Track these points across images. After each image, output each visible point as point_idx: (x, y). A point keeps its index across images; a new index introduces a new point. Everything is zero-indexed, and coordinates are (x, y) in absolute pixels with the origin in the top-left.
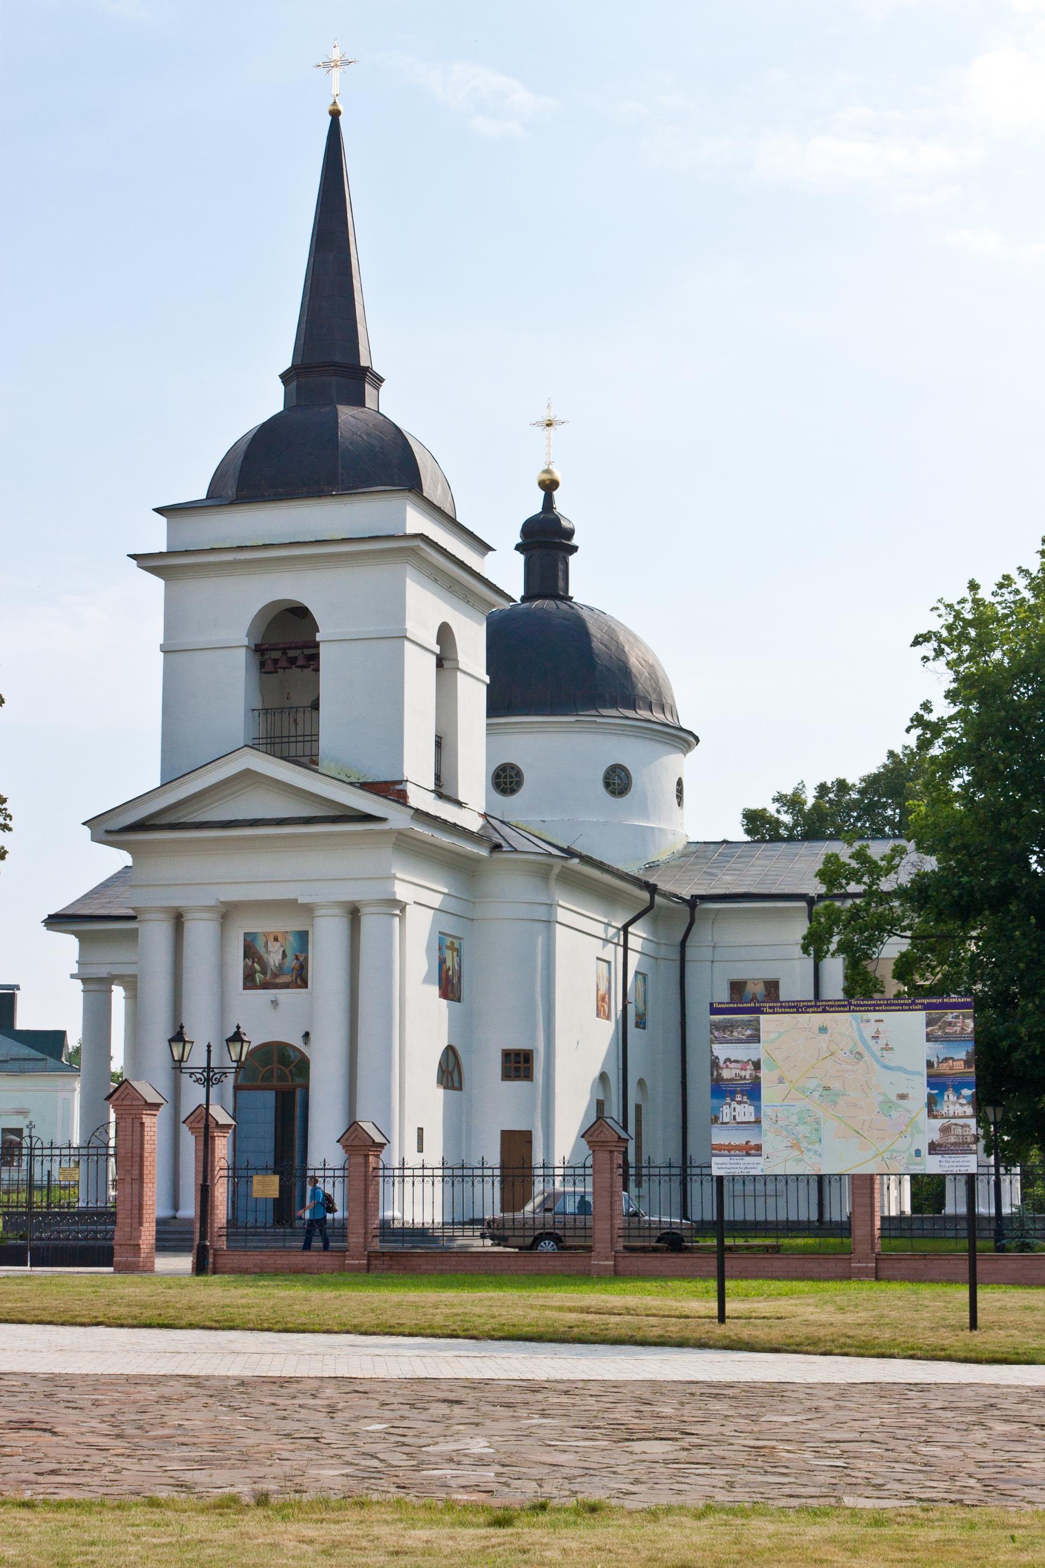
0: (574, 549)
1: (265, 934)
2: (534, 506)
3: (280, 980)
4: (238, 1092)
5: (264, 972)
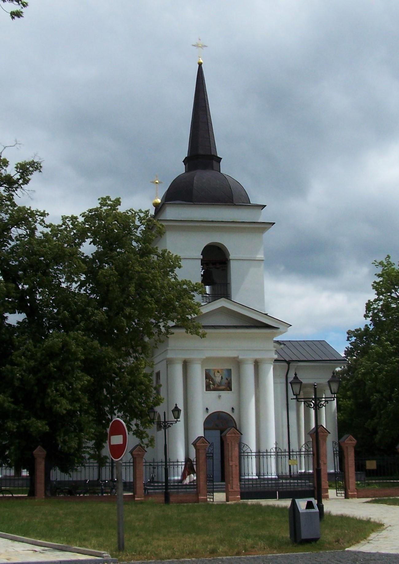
1: (214, 370)
3: (221, 388)
5: (214, 384)
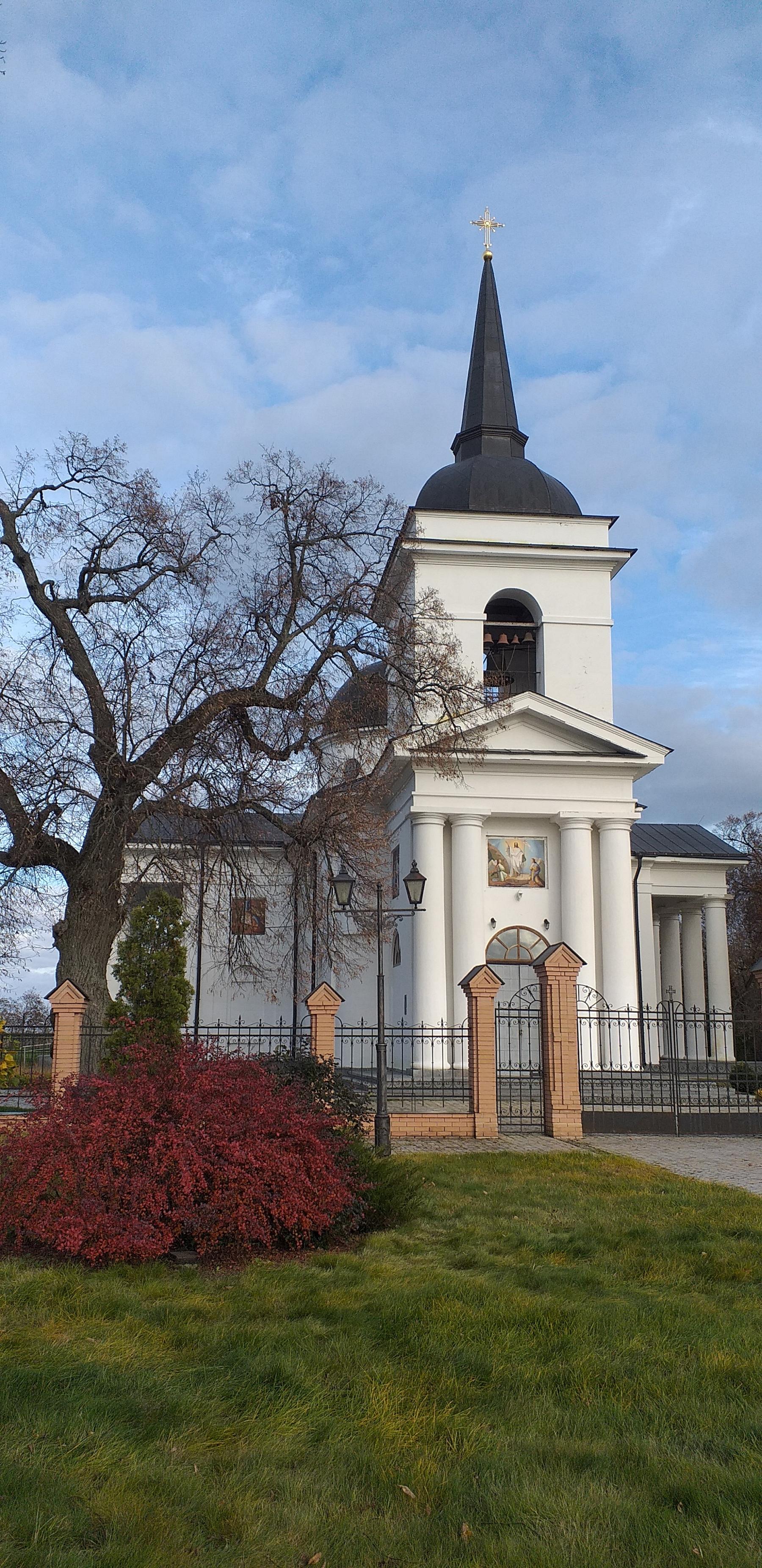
3: (520, 878)
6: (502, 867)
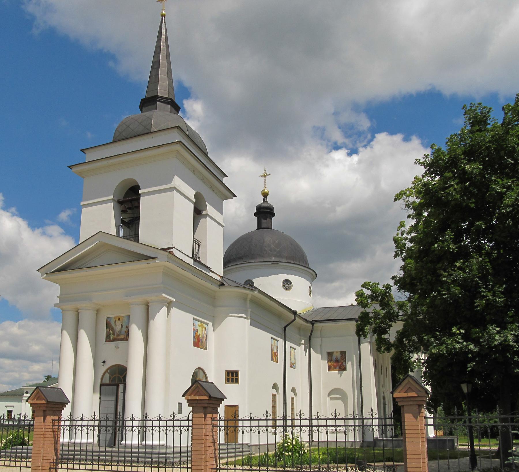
0: (273, 215)
1: (115, 318)
2: (260, 200)
3: (120, 337)
4: (103, 387)
5: (114, 334)
6: (111, 332)
